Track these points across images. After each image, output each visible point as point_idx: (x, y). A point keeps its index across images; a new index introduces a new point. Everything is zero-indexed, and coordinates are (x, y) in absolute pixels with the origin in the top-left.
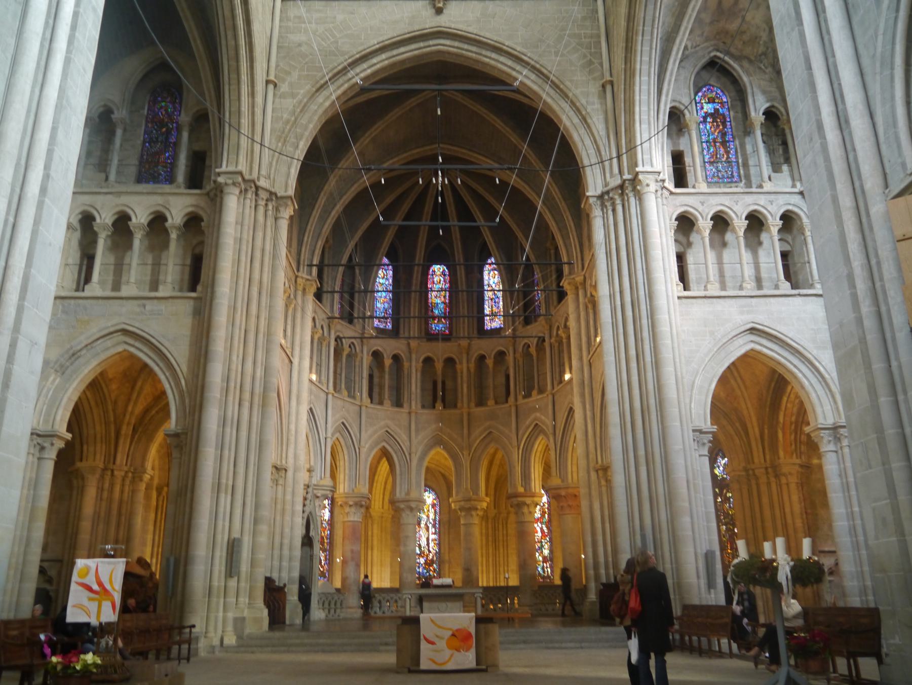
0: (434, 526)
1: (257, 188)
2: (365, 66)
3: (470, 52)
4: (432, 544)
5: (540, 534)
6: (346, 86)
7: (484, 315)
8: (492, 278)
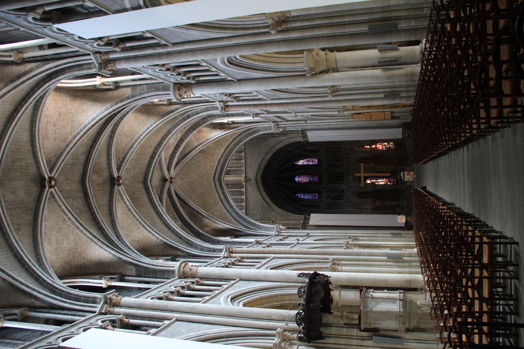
0: (378, 180)
1: (303, 223)
2: (265, 198)
3: (261, 171)
4: (383, 180)
5: (380, 146)
6: (271, 203)
7: (313, 165)
8: (301, 162)
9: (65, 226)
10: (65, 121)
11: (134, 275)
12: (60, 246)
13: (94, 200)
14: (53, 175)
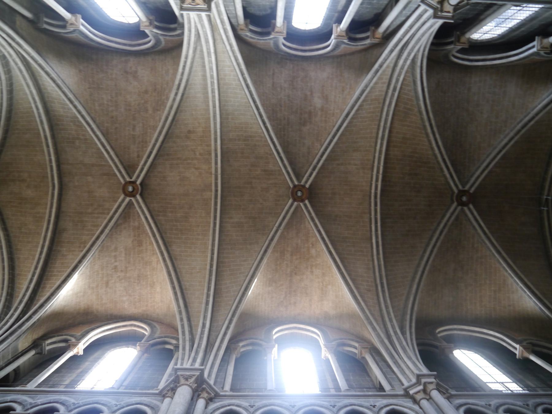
9: (106, 125)
10: (100, 275)
11: (18, 15)
12: (112, 97)
13: (47, 158)
14: (128, 199)
